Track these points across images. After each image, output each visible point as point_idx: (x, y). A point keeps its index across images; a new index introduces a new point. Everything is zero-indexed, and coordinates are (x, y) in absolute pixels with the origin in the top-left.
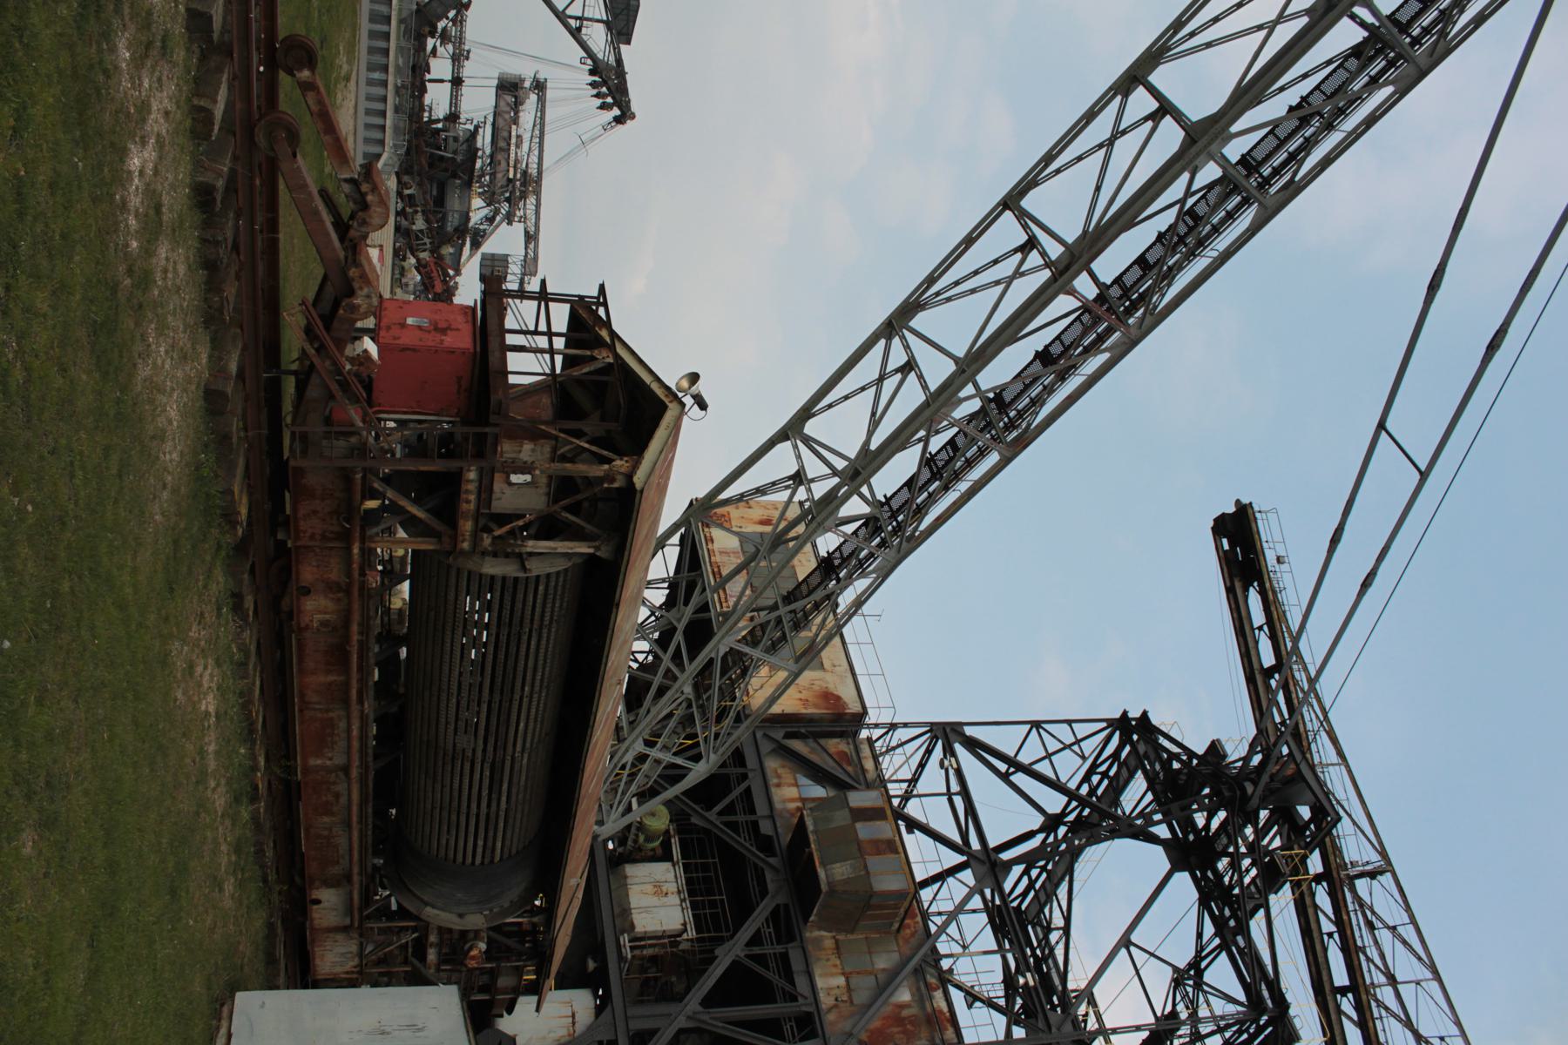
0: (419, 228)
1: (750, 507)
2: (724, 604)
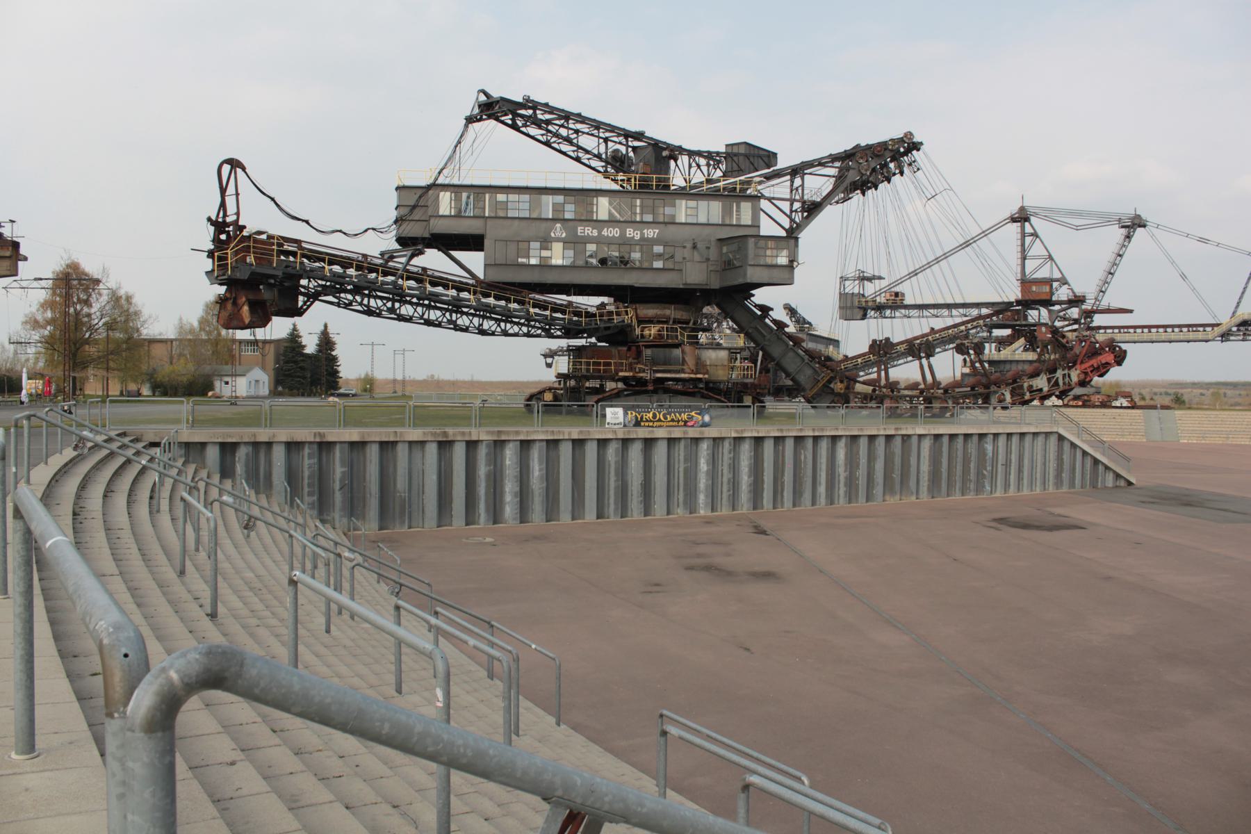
0: (1047, 384)
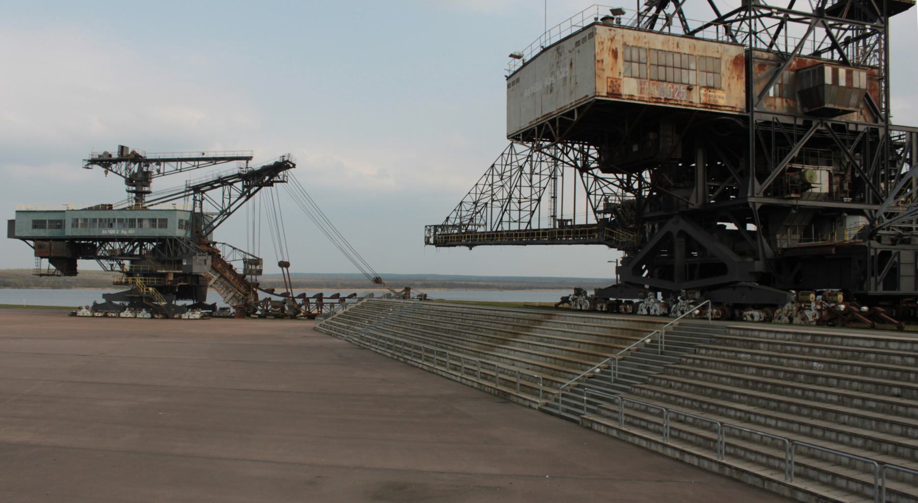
1: (602, 61)
2: (679, 103)
